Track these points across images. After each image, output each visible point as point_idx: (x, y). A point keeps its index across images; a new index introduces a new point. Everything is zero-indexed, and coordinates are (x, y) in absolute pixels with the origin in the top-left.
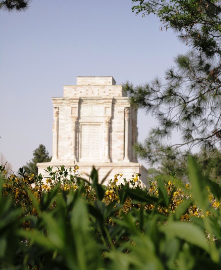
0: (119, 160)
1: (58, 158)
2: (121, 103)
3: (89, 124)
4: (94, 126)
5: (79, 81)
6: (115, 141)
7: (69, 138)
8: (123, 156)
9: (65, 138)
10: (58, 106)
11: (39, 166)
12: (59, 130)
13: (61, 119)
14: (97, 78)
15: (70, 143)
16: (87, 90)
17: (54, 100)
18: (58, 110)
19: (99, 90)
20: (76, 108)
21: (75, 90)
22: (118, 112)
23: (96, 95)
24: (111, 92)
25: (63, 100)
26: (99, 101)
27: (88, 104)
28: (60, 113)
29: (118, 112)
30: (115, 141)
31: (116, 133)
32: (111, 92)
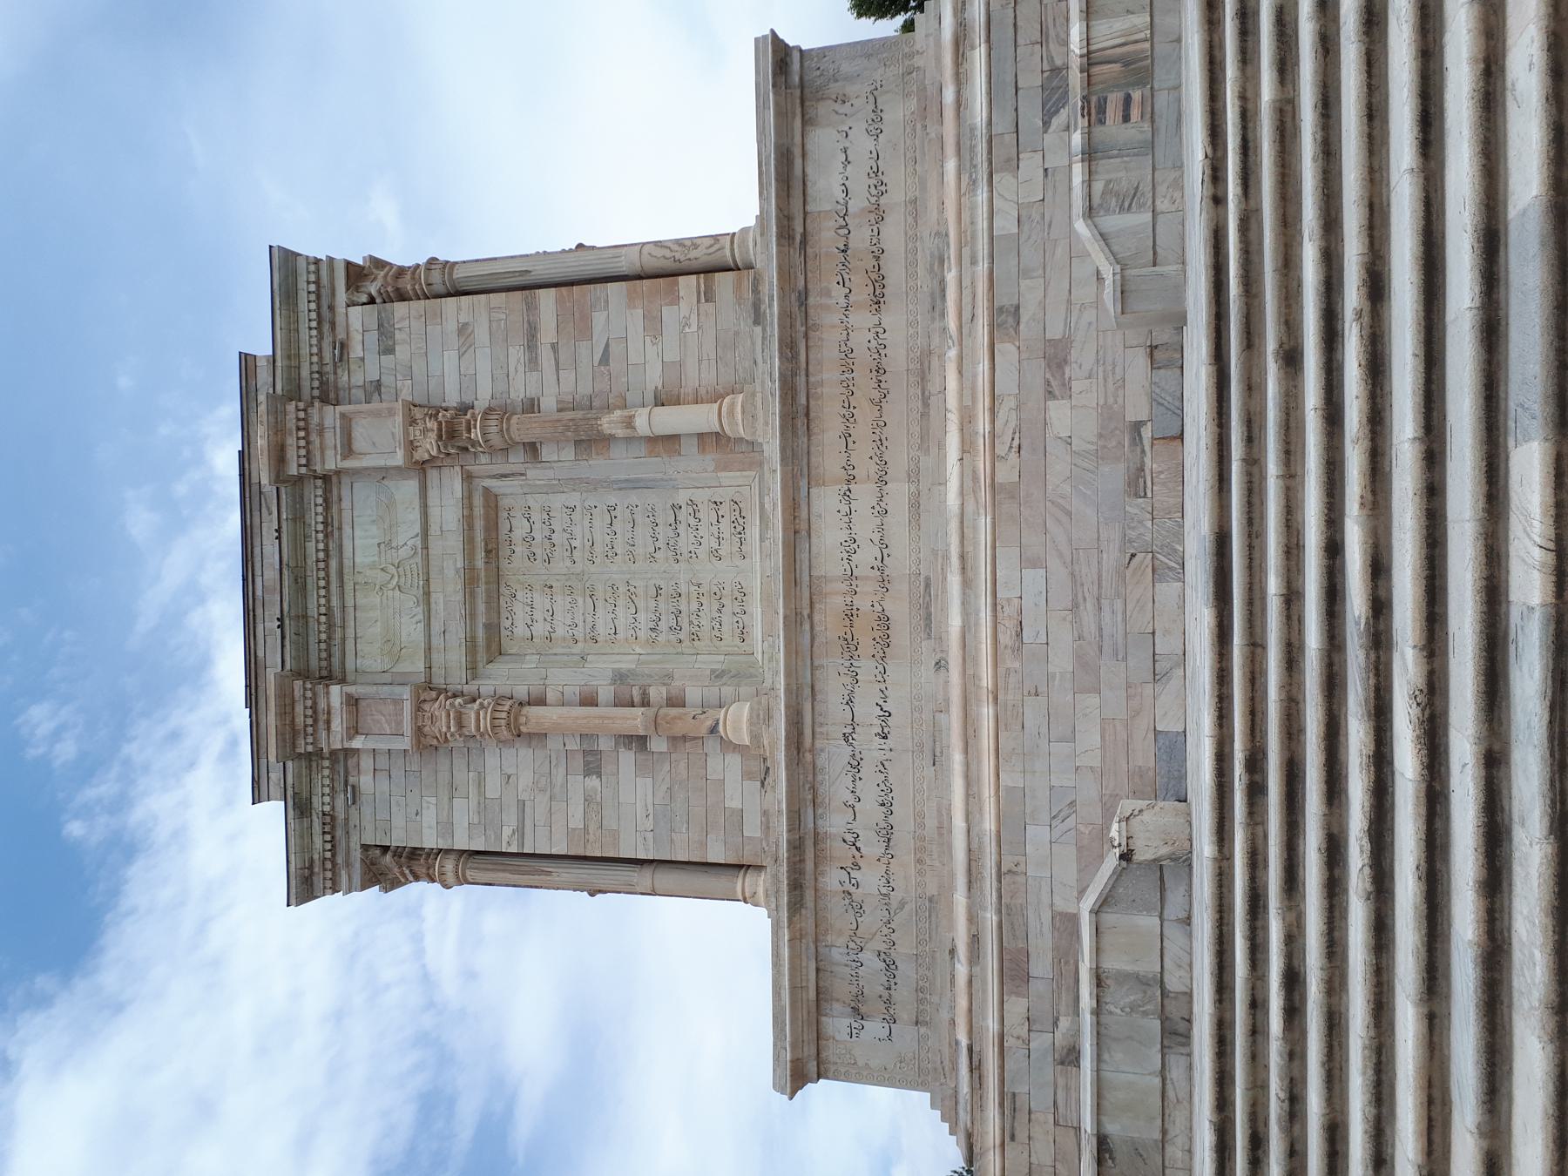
1: (760, 868)
2: (319, 328)
3: (481, 591)
4: (504, 551)
6: (605, 359)
7: (593, 765)
8: (724, 281)
9: (588, 800)
10: (357, 854)
12: (526, 851)
13: (447, 827)
15: (627, 758)
18: (385, 849)
20: (353, 702)
22: (390, 351)
26: (315, 517)
27: (335, 602)
28: (397, 839)
29: (390, 351)
30: (605, 359)
31: (546, 355)
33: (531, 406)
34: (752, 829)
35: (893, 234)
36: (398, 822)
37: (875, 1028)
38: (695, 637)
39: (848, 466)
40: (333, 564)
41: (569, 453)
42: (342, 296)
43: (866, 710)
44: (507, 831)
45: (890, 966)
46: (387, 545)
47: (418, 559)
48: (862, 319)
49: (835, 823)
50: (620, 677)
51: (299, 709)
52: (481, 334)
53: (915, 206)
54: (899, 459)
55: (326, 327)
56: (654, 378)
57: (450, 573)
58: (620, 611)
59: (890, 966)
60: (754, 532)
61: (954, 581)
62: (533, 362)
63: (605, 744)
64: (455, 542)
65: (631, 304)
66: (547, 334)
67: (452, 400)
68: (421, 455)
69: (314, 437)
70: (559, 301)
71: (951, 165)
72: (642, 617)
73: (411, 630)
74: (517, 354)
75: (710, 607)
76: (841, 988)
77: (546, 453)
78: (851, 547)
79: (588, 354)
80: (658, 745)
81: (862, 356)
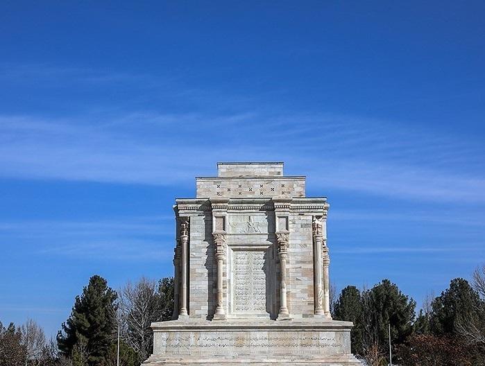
0: (305, 316)
1: (189, 314)
5: (223, 170)
6: (297, 279)
9: (202, 274)
10: (188, 215)
11: (155, 328)
13: (195, 239)
14: (257, 166)
16: (240, 186)
17: (182, 203)
19: (262, 186)
21: (218, 187)
23: (257, 194)
24: (285, 189)
25: (197, 203)
32: (285, 189)
33: (288, 262)
34: (197, 312)
35: (314, 349)
36: (196, 226)
37: (165, 343)
38: (237, 298)
39: (271, 339)
40: (254, 211)
41: (277, 271)
42: (315, 214)
43: (225, 342)
44: (194, 254)
45: (177, 346)
46: (258, 225)
47: (255, 232)
48: (299, 342)
49: (203, 335)
50: (229, 280)
51: (222, 204)
52: (305, 250)
53: (319, 353)
54: (272, 349)
55: (308, 210)
56: (293, 291)
57: (252, 240)
58: (243, 280)
59: (177, 346)
60: (260, 312)
61: (249, 361)
62: (297, 262)
63: (214, 278)
64: (258, 242)
65: (310, 286)
66: (303, 266)
67: (290, 242)
68: (278, 236)
69: (283, 209)
70: (310, 269)
71: (323, 361)
72: (242, 285)
73: (239, 230)
74: (299, 258)
75: (243, 302)
76: (172, 335)
77: (278, 265)
78: (256, 339)
79: (299, 276)
80: (214, 290)
81: (292, 342)
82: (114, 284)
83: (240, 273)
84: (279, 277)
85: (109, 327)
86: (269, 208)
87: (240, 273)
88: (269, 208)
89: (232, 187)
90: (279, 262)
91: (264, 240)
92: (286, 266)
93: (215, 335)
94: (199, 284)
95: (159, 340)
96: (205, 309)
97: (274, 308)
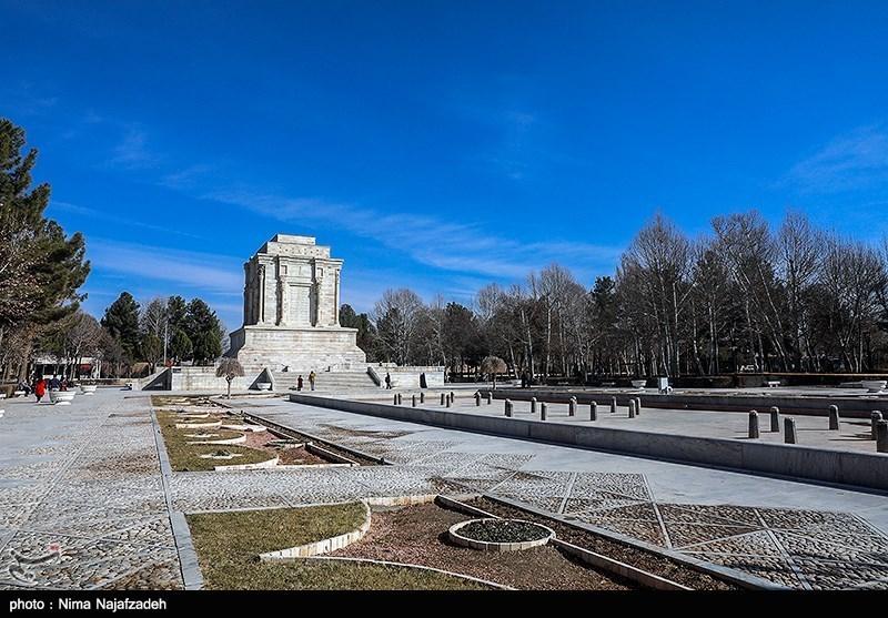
73: (294, 275)
82: (136, 299)
83: (296, 299)
84: (317, 303)
85: (135, 326)
86: (312, 262)
87: (296, 299)
88: (312, 262)
89: (289, 249)
90: (317, 294)
91: (309, 281)
92: (321, 297)
93: (282, 334)
94: (270, 305)
95: (249, 336)
96: (274, 319)
97: (314, 321)
